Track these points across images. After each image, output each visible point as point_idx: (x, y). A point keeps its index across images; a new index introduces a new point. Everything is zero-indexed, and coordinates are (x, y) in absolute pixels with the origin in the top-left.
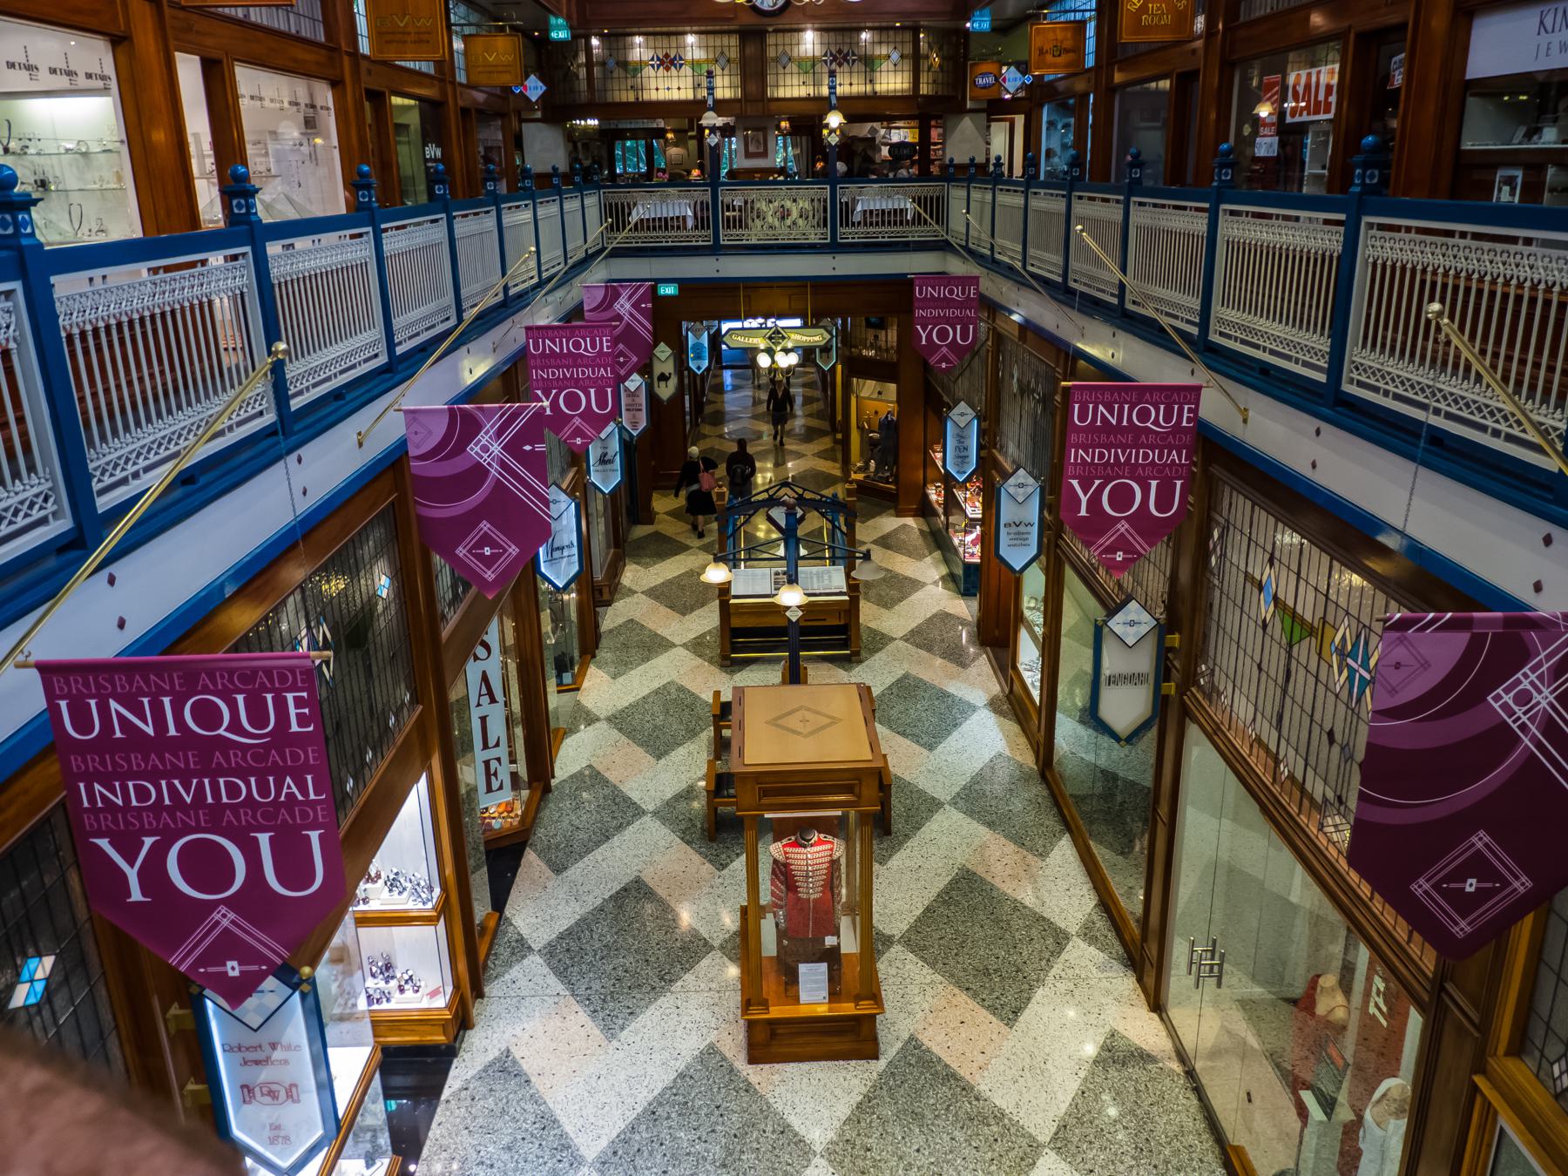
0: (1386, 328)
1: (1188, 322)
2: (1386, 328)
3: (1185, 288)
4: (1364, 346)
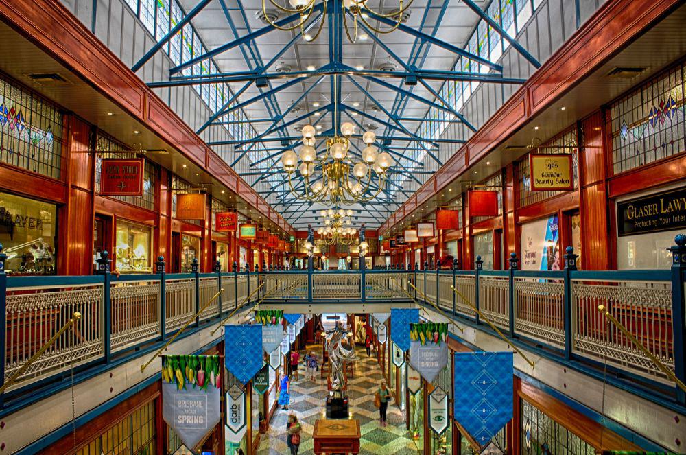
0: (589, 326)
1: (505, 325)
2: (589, 326)
3: (501, 311)
4: (578, 333)
